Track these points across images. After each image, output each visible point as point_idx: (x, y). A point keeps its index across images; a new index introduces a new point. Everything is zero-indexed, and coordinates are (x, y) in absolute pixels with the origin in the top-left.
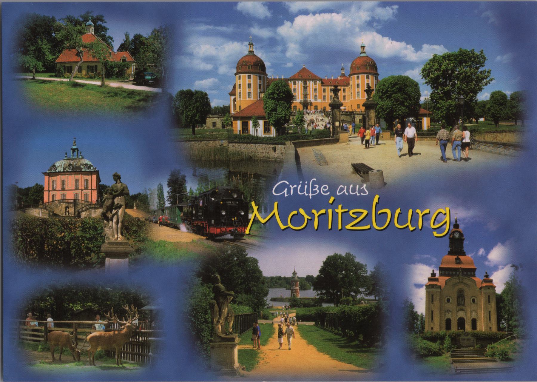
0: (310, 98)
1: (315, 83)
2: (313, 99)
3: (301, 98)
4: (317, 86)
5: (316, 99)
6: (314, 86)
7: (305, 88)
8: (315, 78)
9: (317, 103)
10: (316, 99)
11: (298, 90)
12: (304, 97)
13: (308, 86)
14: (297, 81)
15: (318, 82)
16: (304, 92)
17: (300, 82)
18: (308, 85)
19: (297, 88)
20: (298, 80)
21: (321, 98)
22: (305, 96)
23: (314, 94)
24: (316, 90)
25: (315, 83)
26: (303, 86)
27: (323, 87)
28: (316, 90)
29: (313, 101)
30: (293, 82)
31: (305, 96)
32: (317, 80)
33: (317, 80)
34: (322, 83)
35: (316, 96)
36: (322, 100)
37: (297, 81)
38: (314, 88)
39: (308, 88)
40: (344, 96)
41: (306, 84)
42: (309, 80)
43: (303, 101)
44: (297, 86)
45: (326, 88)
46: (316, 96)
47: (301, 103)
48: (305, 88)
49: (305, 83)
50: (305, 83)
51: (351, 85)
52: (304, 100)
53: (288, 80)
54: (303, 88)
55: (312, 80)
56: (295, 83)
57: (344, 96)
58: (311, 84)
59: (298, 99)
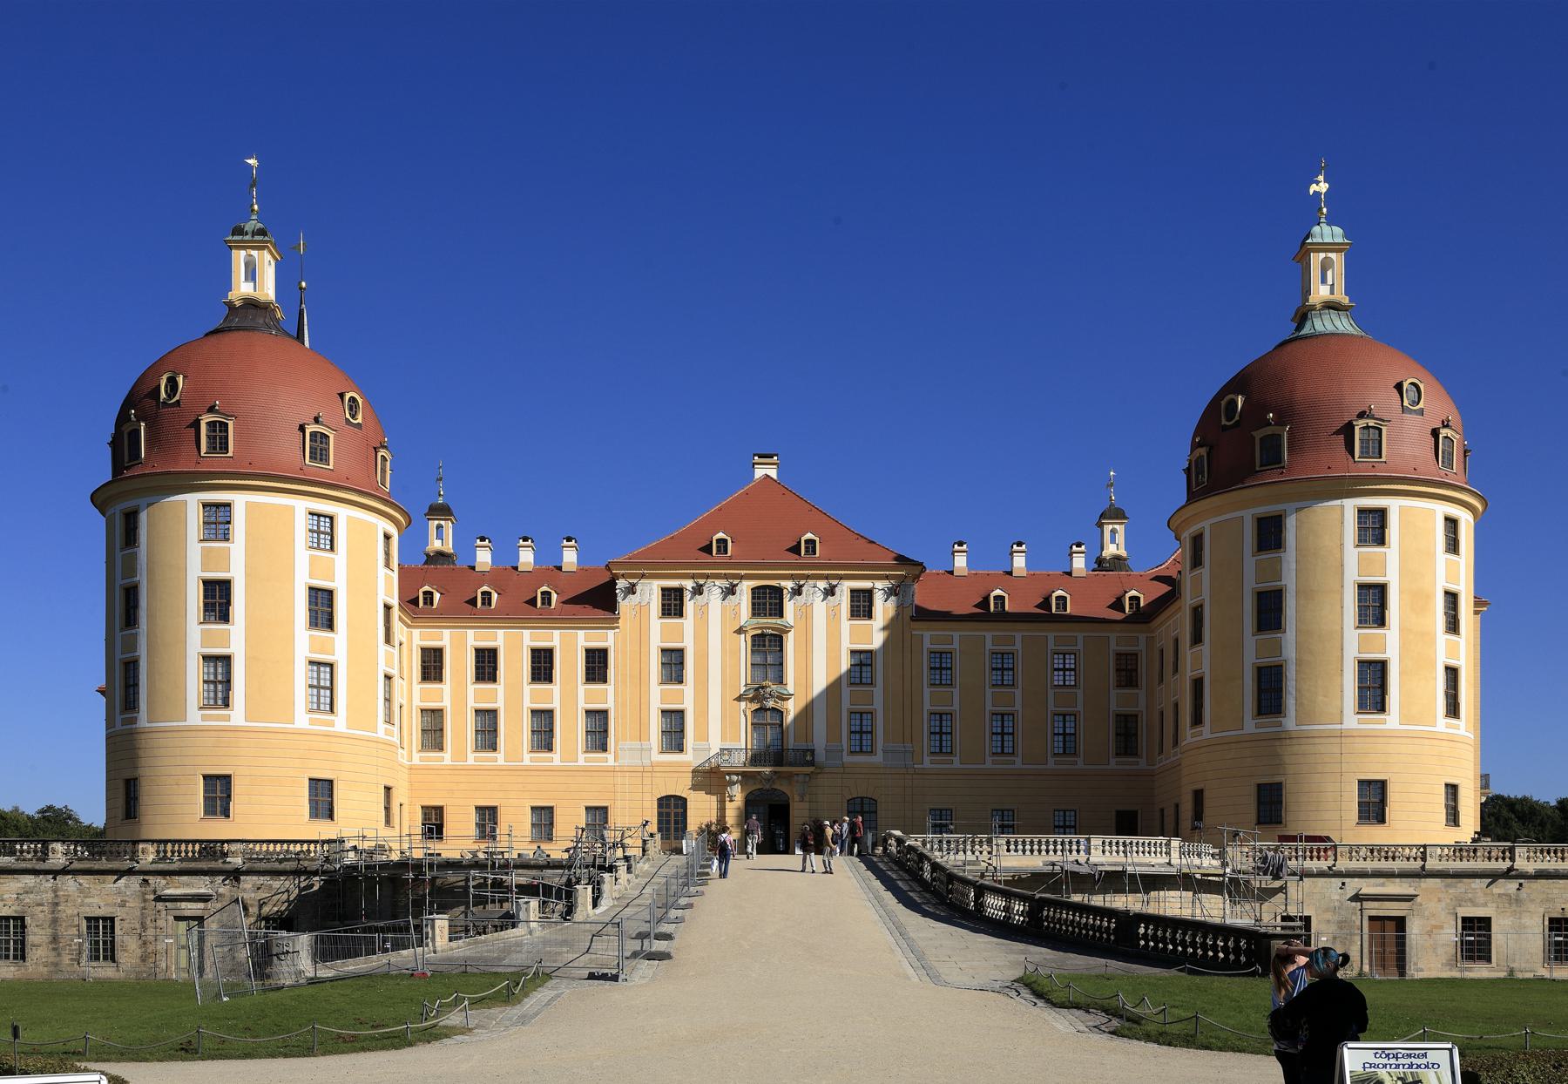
11: (703, 656)
39: (790, 642)
49: (768, 601)
50: (768, 601)
54: (744, 644)
56: (673, 604)
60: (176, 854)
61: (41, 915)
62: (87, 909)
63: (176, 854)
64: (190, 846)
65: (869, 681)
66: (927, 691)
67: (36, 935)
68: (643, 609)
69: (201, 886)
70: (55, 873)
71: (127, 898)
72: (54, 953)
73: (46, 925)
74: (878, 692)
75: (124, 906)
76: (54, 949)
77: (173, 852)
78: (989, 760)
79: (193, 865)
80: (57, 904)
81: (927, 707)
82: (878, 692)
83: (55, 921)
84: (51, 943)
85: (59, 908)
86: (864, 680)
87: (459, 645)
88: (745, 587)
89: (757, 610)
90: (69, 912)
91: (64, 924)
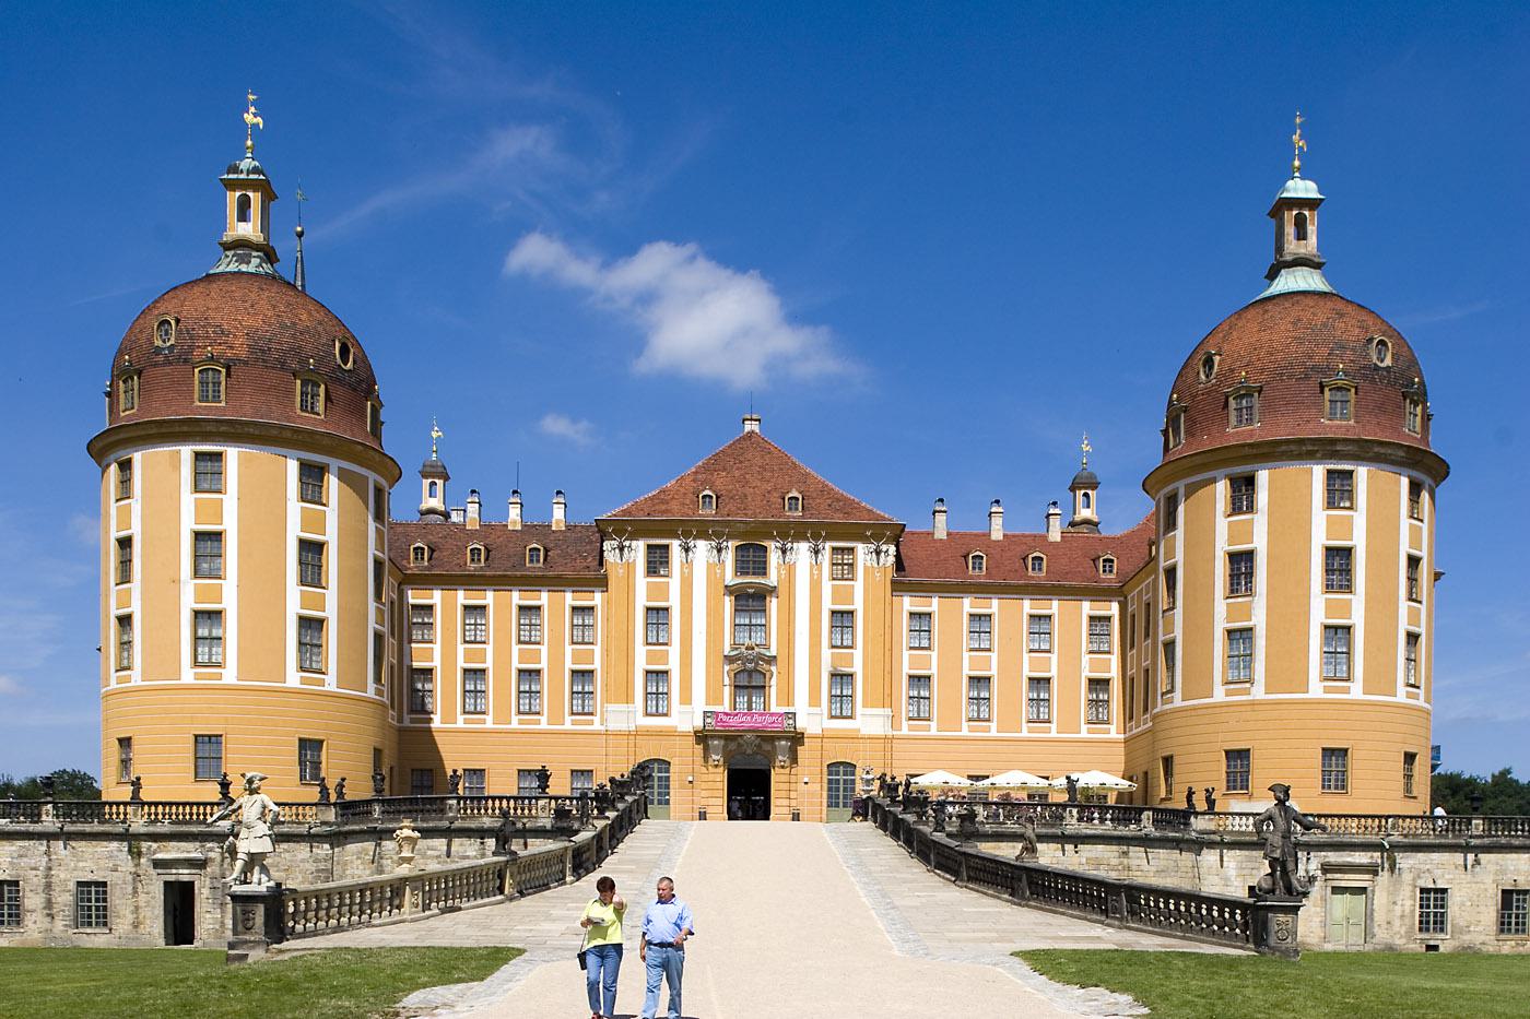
0: (788, 696)
1: (844, 568)
2: (814, 700)
3: (713, 695)
4: (859, 586)
6: (827, 586)
7: (750, 600)
8: (838, 519)
9: (854, 737)
13: (773, 590)
17: (702, 547)
18: (772, 578)
20: (691, 530)
21: (888, 700)
22: (750, 675)
23: (826, 653)
24: (842, 618)
25: (844, 568)
26: (729, 590)
27: (908, 603)
28: (842, 618)
29: (811, 720)
30: (639, 547)
31: (750, 675)
32: (858, 533)
35: (841, 678)
36: (894, 720)
37: (675, 545)
38: (827, 605)
39: (773, 604)
41: (762, 570)
42: (791, 532)
44: (675, 583)
45: (934, 604)
46: (841, 678)
47: (702, 737)
48: (750, 600)
49: (751, 559)
50: (751, 559)
54: (728, 603)
55: (812, 532)
56: (657, 561)
59: (686, 699)
60: (167, 817)
61: (35, 879)
62: (80, 873)
63: (167, 817)
64: (188, 808)
65: (850, 643)
66: (906, 654)
67: (32, 900)
68: (630, 567)
69: (191, 850)
70: (49, 836)
71: (119, 863)
72: (49, 919)
73: (40, 889)
74: (858, 654)
75: (116, 871)
76: (48, 915)
77: (164, 815)
78: (965, 725)
79: (184, 828)
80: (50, 869)
82: (858, 654)
83: (48, 886)
84: (45, 908)
85: (53, 872)
86: (845, 644)
87: (448, 606)
88: (732, 544)
89: (741, 568)
90: (62, 876)
91: (58, 889)
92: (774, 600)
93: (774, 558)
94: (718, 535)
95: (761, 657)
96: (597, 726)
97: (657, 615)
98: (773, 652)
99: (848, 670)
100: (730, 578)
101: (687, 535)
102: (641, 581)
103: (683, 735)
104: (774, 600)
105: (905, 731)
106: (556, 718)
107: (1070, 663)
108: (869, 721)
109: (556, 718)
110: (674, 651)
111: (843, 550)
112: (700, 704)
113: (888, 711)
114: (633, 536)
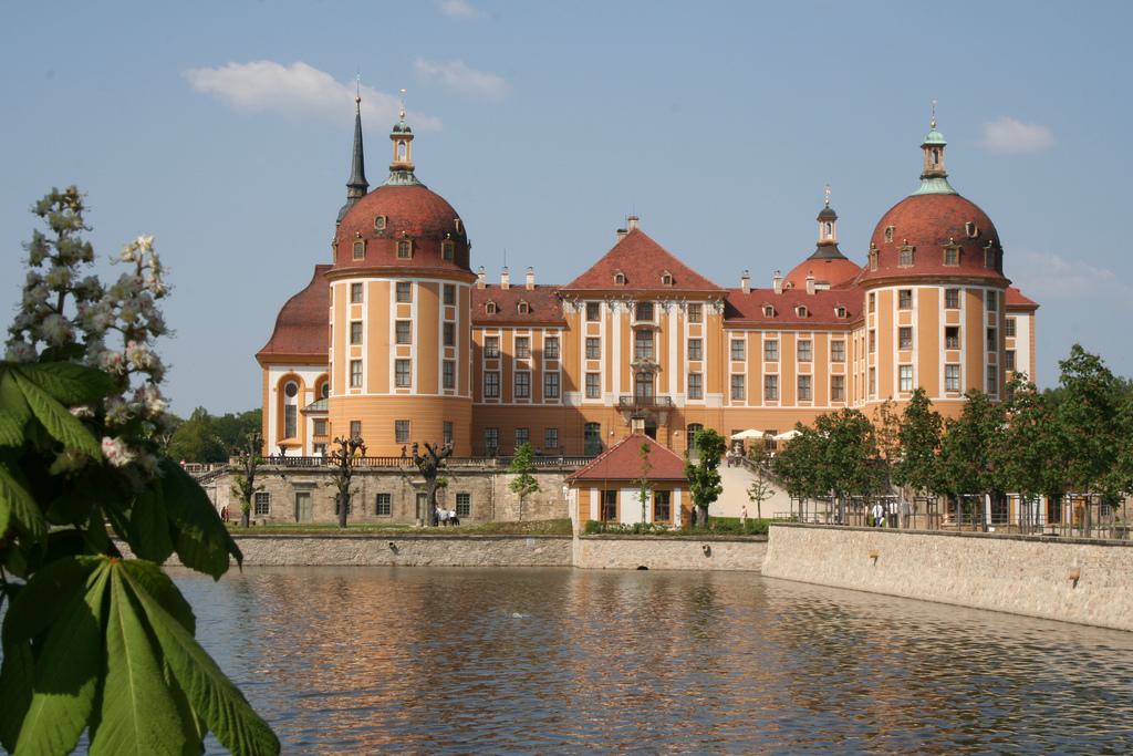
0: (665, 387)
1: (694, 314)
2: (680, 389)
3: (624, 387)
5: (694, 390)
6: (687, 325)
7: (644, 334)
8: (692, 288)
9: (702, 409)
10: (694, 390)
12: (637, 382)
14: (604, 307)
15: (707, 309)
16: (637, 358)
17: (619, 307)
18: (657, 321)
19: (602, 335)
20: (611, 296)
21: (721, 388)
22: (645, 374)
23: (687, 363)
24: (695, 344)
25: (694, 314)
28: (695, 344)
29: (680, 399)
31: (645, 374)
32: (704, 296)
33: (705, 298)
34: (731, 313)
35: (695, 377)
36: (725, 401)
39: (657, 336)
40: (837, 379)
41: (650, 317)
43: (630, 402)
44: (602, 324)
46: (695, 377)
47: (620, 408)
48: (644, 334)
49: (644, 311)
50: (644, 311)
51: (872, 332)
52: (636, 398)
53: (561, 295)
54: (632, 335)
55: (677, 296)
56: (593, 312)
57: (837, 379)
58: (671, 317)
59: (609, 388)
66: (730, 363)
68: (578, 314)
74: (704, 363)
81: (730, 372)
82: (704, 363)
92: (658, 334)
93: (658, 309)
94: (626, 298)
95: (651, 365)
96: (560, 404)
97: (593, 344)
98: (657, 363)
99: (699, 372)
100: (633, 321)
101: (609, 298)
102: (584, 323)
103: (608, 409)
104: (658, 334)
105: (730, 406)
106: (537, 399)
107: (821, 367)
108: (710, 400)
109: (537, 399)
110: (602, 362)
111: (695, 305)
112: (617, 392)
113: (721, 395)
114: (580, 300)
